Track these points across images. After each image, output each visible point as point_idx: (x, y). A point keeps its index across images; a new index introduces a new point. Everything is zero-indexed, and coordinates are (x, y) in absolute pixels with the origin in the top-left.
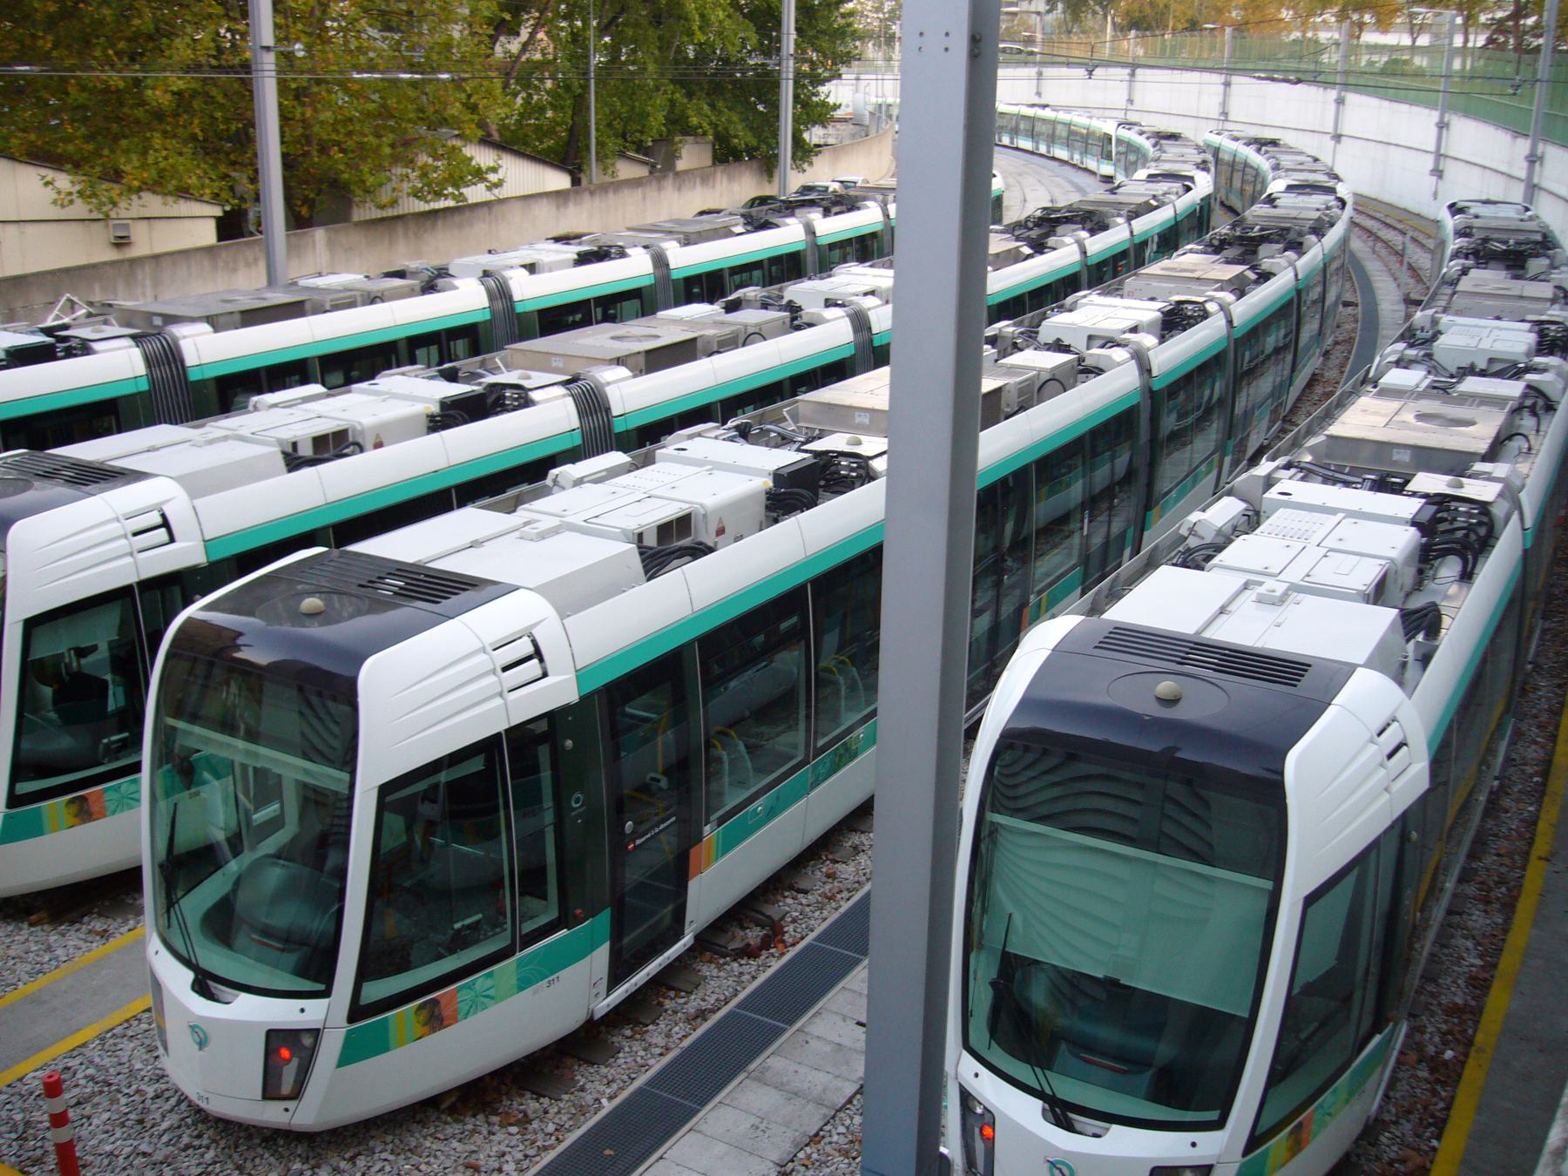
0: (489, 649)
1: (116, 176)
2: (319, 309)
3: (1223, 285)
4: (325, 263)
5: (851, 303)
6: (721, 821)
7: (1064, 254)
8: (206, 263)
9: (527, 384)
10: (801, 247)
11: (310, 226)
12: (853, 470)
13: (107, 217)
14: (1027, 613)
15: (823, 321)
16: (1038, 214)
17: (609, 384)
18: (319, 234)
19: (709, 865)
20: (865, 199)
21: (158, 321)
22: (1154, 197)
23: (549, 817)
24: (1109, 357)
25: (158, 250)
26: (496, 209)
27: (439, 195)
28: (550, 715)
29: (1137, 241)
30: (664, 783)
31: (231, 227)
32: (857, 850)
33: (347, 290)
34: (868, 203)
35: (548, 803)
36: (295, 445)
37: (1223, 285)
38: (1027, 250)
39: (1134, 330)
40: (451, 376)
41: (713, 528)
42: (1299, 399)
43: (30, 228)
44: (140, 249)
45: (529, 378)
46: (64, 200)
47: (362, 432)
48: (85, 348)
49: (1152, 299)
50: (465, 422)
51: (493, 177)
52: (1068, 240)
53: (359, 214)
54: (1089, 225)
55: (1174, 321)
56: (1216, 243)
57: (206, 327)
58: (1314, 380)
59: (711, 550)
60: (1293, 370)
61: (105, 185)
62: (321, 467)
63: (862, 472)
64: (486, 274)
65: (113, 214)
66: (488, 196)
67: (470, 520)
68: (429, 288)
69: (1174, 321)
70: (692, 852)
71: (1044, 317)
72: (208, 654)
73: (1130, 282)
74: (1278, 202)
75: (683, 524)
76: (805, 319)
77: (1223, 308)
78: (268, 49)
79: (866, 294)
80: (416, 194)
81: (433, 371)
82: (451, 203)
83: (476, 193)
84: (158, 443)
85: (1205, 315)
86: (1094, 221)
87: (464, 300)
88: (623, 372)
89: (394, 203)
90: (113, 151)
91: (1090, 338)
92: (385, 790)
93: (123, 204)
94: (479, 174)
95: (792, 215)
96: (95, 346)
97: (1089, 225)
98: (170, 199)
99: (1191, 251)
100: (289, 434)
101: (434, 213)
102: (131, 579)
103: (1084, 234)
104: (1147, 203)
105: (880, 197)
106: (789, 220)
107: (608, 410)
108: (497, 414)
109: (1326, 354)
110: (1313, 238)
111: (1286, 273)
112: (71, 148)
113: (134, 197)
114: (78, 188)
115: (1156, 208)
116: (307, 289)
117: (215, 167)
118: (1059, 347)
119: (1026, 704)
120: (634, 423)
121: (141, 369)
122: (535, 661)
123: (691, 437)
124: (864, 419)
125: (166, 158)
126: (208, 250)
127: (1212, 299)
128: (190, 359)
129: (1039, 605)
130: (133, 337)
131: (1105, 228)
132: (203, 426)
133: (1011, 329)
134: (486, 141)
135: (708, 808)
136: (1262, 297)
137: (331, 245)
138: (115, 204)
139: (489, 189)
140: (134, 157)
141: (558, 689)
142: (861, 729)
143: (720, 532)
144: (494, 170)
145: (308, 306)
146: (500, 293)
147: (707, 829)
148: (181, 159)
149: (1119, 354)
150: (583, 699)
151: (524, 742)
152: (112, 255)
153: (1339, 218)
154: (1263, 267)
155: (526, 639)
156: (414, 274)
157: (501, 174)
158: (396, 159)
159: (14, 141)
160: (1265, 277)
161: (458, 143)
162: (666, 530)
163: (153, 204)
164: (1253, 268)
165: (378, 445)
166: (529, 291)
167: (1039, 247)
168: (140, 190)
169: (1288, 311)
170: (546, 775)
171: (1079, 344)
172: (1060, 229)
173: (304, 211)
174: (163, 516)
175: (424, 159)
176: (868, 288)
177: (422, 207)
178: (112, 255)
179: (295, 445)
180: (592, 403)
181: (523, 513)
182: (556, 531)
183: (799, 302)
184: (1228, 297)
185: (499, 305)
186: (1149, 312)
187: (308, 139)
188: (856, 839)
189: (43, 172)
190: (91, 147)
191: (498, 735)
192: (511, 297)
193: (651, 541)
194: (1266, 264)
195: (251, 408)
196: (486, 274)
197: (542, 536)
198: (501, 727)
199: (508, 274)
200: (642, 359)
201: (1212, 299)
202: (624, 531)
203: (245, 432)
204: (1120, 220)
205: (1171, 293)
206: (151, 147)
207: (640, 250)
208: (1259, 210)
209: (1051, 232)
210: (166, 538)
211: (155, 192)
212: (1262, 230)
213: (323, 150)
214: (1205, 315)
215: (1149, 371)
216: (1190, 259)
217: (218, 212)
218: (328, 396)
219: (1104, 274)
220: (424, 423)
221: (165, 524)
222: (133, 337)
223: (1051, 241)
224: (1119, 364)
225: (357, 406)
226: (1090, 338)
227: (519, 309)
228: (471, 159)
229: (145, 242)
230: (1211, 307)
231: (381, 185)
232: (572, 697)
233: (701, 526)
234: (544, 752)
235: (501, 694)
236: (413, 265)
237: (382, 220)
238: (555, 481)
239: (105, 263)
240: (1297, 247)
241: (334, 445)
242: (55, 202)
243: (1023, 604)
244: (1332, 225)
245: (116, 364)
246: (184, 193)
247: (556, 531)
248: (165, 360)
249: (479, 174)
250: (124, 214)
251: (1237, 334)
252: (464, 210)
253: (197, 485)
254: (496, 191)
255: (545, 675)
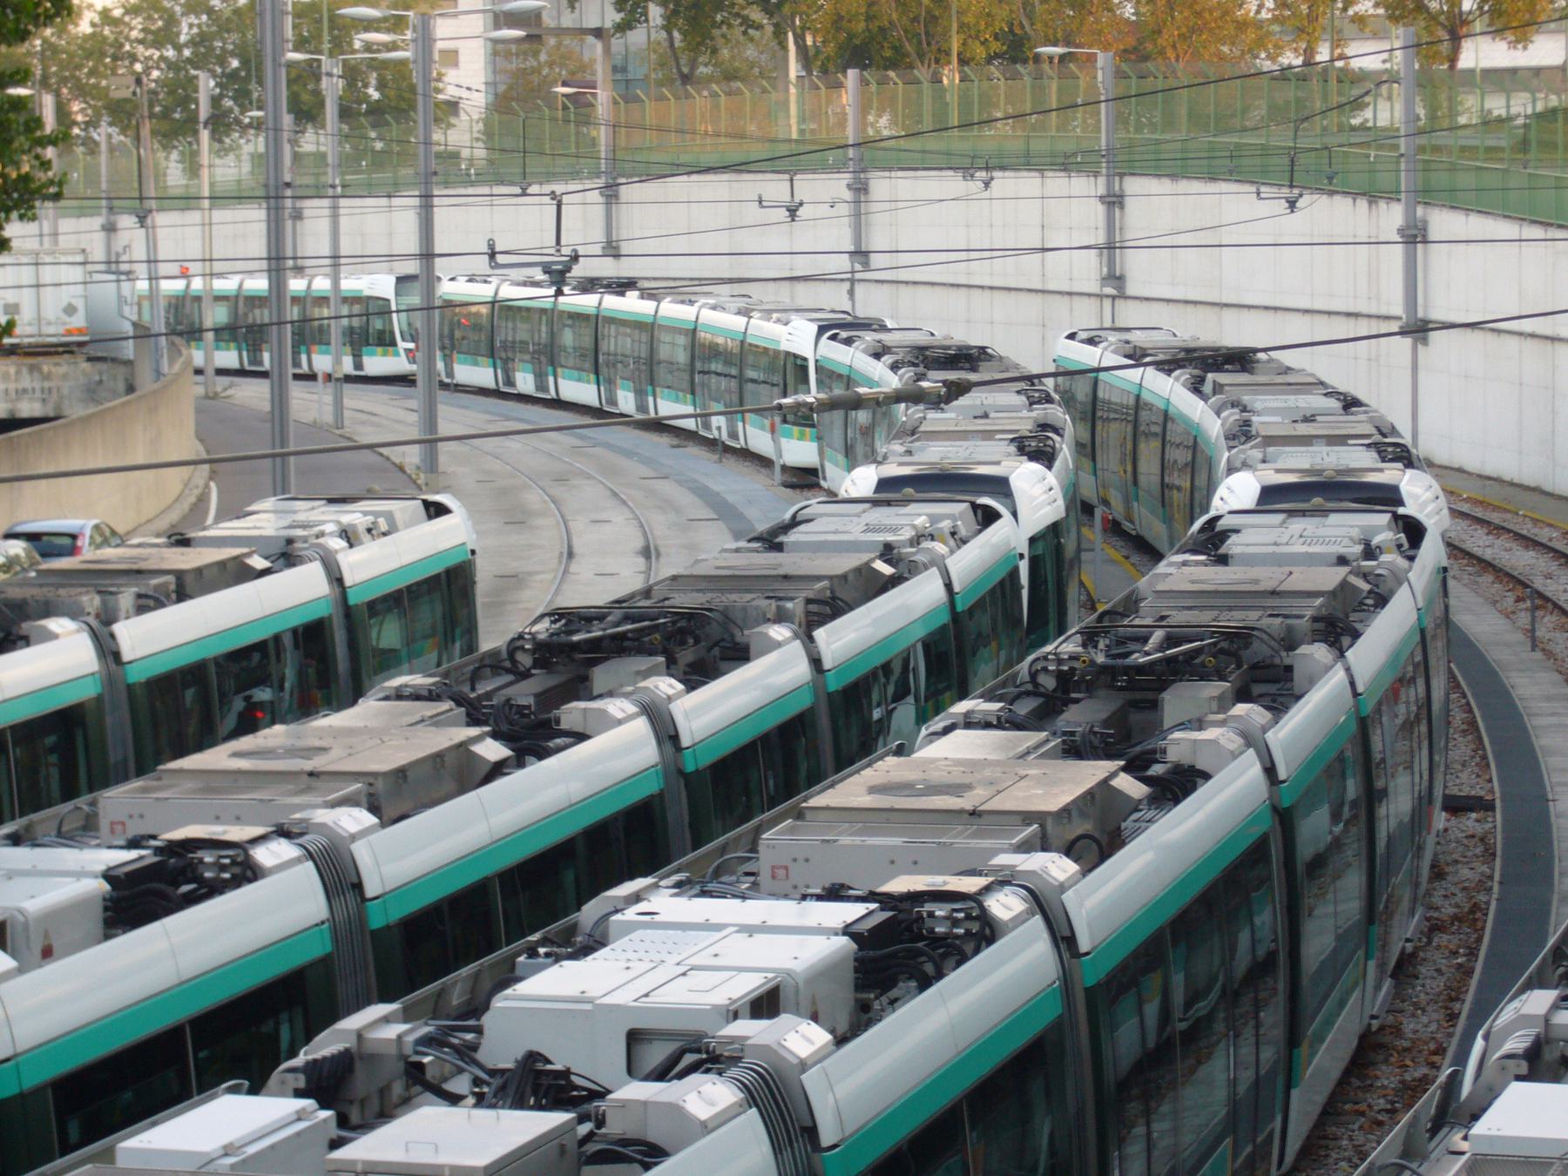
3: (1044, 832)
7: (610, 751)
16: (543, 629)
20: (48, 610)
22: (888, 552)
24: (676, 1111)
29: (834, 684)
34: (55, 624)
37: (1044, 832)
38: (492, 750)
39: (766, 1004)
42: (1330, 1112)
49: (835, 893)
52: (617, 707)
54: (686, 656)
55: (900, 951)
56: (1049, 683)
58: (1369, 1049)
60: (1293, 1038)
69: (900, 951)
71: (508, 977)
73: (778, 839)
74: (1233, 545)
77: (1043, 903)
85: (986, 932)
86: (697, 639)
91: (635, 1038)
97: (686, 656)
99: (969, 723)
103: (666, 685)
104: (865, 571)
105: (91, 602)
109: (1404, 969)
110: (1319, 652)
111: (1237, 764)
115: (894, 581)
118: (536, 1083)
127: (1005, 880)
131: (741, 655)
133: (392, 1031)
136: (1168, 848)
149: (706, 1096)
153: (1400, 579)
154: (1173, 755)
160: (1178, 784)
164: (1136, 767)
167: (533, 737)
169: (1258, 873)
171: (591, 1058)
172: (601, 676)
184: (1058, 867)
186: (804, 936)
194: (1179, 745)
201: (1005, 880)
204: (779, 632)
205: (894, 867)
208: (1180, 572)
209: (578, 688)
212: (1171, 641)
214: (986, 932)
215: (812, 1132)
216: (960, 751)
219: (699, 819)
223: (572, 713)
224: (706, 1128)
226: (635, 1038)
230: (1004, 905)
240: (1272, 684)
244: (1382, 601)
251: (1091, 974)
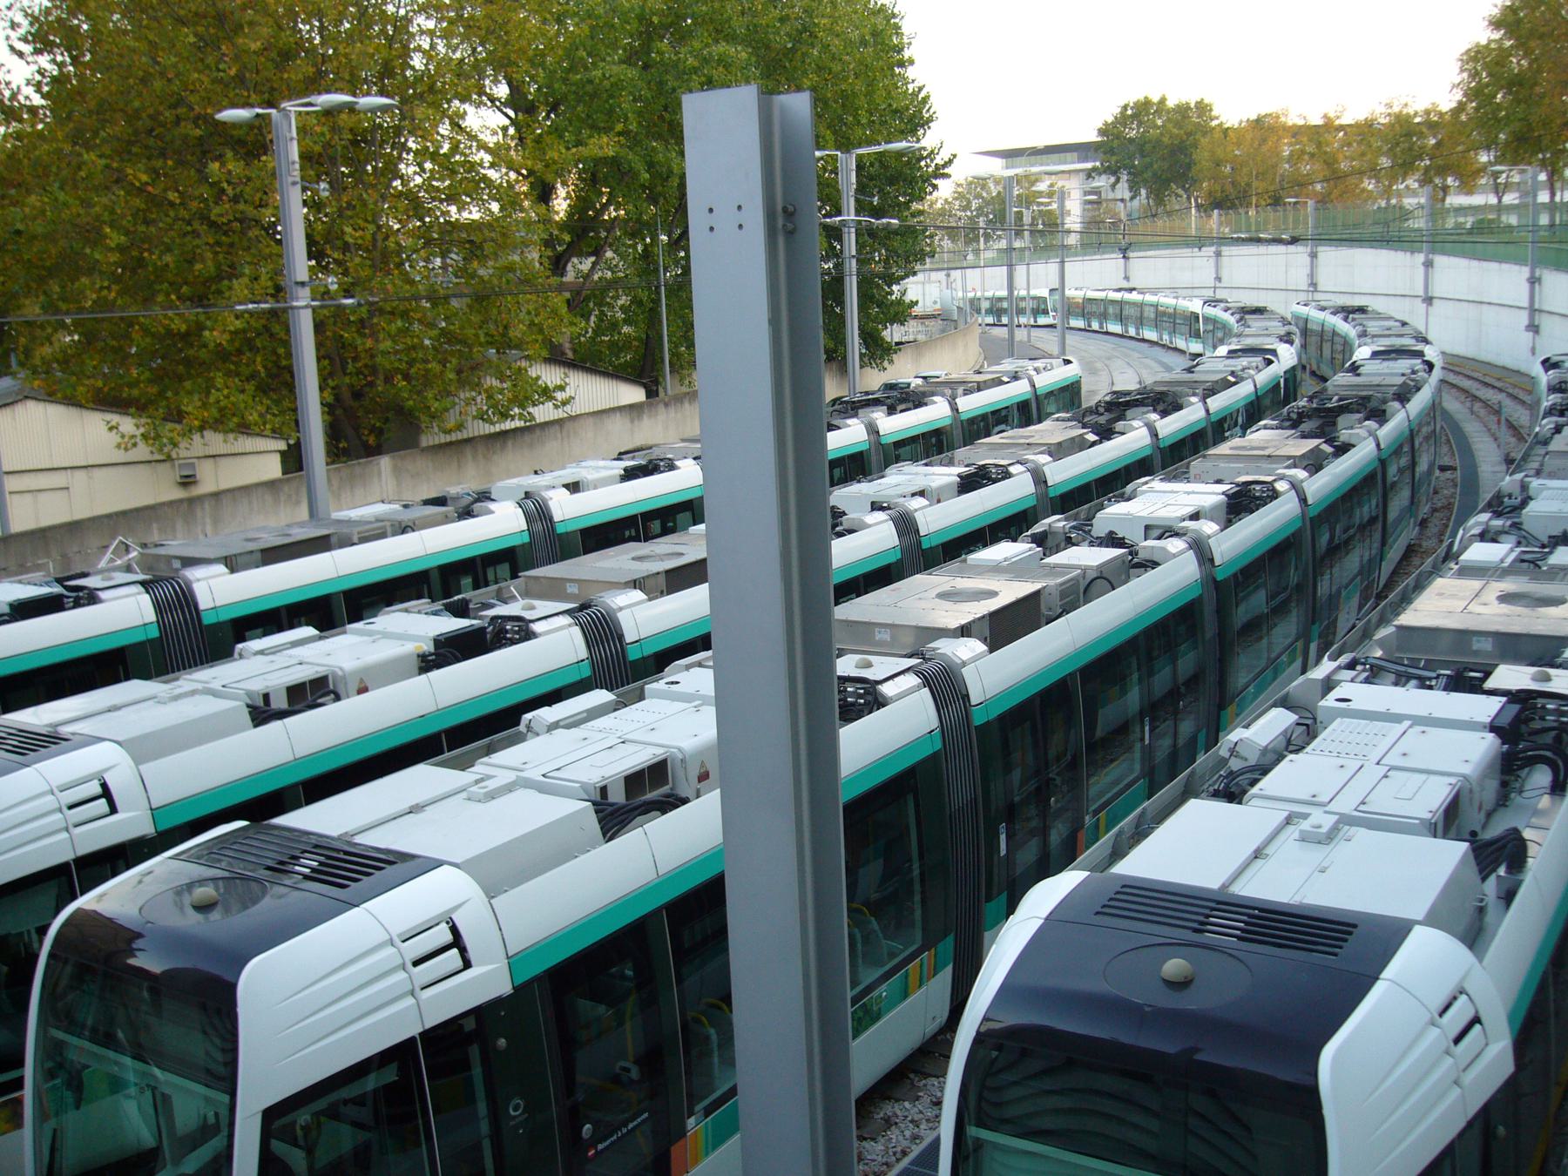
0: (397, 941)
1: (177, 416)
2: (346, 542)
3: (1295, 462)
4: (377, 492)
5: (897, 505)
6: (708, 1112)
7: (1133, 438)
8: (268, 498)
9: (528, 615)
10: (865, 447)
11: (380, 453)
12: (860, 696)
13: (169, 458)
14: (1082, 836)
15: (866, 526)
16: (1108, 398)
17: (621, 609)
18: (385, 462)
19: (696, 1162)
20: (933, 394)
21: (177, 564)
22: (1233, 373)
23: (484, 1127)
24: (1164, 549)
25: (224, 485)
26: (568, 425)
27: (505, 416)
28: (477, 1012)
29: (1214, 419)
30: (635, 1073)
31: (294, 460)
32: (889, 1123)
33: (378, 520)
34: (935, 398)
35: (482, 1108)
36: (266, 697)
37: (1295, 462)
38: (1092, 437)
39: (1195, 516)
40: (460, 610)
41: (694, 773)
42: (1395, 573)
43: (97, 473)
44: (207, 486)
45: (533, 608)
46: (128, 444)
47: (344, 677)
48: (91, 598)
49: (1218, 482)
50: (459, 661)
51: (560, 396)
52: (1136, 423)
53: (426, 440)
54: (1160, 407)
55: (1241, 503)
56: (1294, 416)
57: (221, 568)
58: (1410, 551)
59: (685, 801)
60: (1383, 543)
61: (170, 426)
62: (287, 721)
63: (870, 698)
64: (528, 495)
65: (174, 455)
66: (560, 414)
67: (422, 779)
68: (466, 513)
69: (1241, 503)
70: (675, 1150)
71: (1102, 507)
72: (100, 947)
73: (1196, 464)
74: (1361, 370)
75: (658, 772)
76: (846, 525)
77: (1295, 486)
78: (303, 284)
79: (913, 495)
80: (482, 417)
81: (438, 606)
82: (518, 423)
83: (544, 412)
84: (117, 701)
85: (1274, 495)
86: (1164, 401)
87: (502, 523)
88: (638, 595)
89: (460, 427)
90: (176, 393)
91: (1147, 528)
92: (272, 1116)
93: (182, 445)
94: (547, 393)
95: (856, 416)
96: (102, 595)
97: (1160, 407)
98: (231, 436)
99: (1265, 427)
100: (258, 686)
101: (504, 434)
102: (67, 856)
103: (1154, 416)
104: (1225, 380)
105: (948, 392)
106: (849, 421)
107: (621, 637)
108: (499, 648)
109: (1423, 524)
110: (1396, 405)
111: (1365, 445)
112: (135, 392)
113: (197, 437)
114: (142, 430)
115: (1235, 384)
116: (339, 522)
117: (277, 402)
118: (1112, 540)
119: (1007, 991)
120: (649, 650)
121: (150, 615)
122: (455, 951)
123: (688, 667)
124: (885, 636)
125: (227, 397)
126: (271, 485)
127: (1282, 477)
128: (204, 602)
129: (1097, 826)
130: (143, 583)
131: (1179, 408)
132: (177, 679)
133: (1061, 524)
134: (556, 357)
135: (690, 1096)
136: (1340, 471)
137: (397, 471)
138: (175, 445)
139: (556, 407)
140: (196, 397)
141: (487, 980)
142: (884, 986)
143: (704, 777)
144: (561, 388)
145: (334, 540)
146: (538, 513)
147: (691, 1121)
148: (241, 396)
149: (1175, 545)
150: (519, 990)
151: (448, 1045)
152: (179, 494)
153: (1425, 381)
154: (1342, 439)
155: (444, 925)
156: (456, 498)
157: (569, 392)
158: (462, 383)
159: (81, 389)
160: (1342, 449)
161: (524, 364)
162: (635, 781)
163: (215, 441)
164: (1329, 441)
165: (363, 690)
166: (567, 509)
167: (1106, 433)
168: (202, 429)
169: (1370, 483)
170: (477, 1071)
171: (1134, 535)
172: (1129, 413)
173: (372, 440)
174: (104, 786)
175: (491, 382)
176: (916, 489)
177: (489, 429)
178: (179, 494)
179: (266, 697)
180: (601, 631)
181: (480, 768)
182: (509, 788)
183: (842, 507)
184: (1301, 474)
185: (538, 527)
186: (1210, 495)
187: (374, 370)
188: (888, 1109)
189: (109, 416)
190: (154, 390)
191: (412, 1039)
192: (551, 519)
193: (617, 796)
194: (1344, 435)
195: (236, 655)
196: (528, 495)
197: (492, 796)
198: (414, 1030)
199: (548, 494)
200: (662, 579)
201: (1282, 477)
202: (584, 786)
203: (216, 685)
204: (1194, 399)
205: (1239, 474)
206: (214, 387)
207: (690, 461)
208: (1341, 379)
209: (1122, 417)
210: (106, 809)
211: (216, 430)
212: (1340, 400)
213: (388, 379)
214: (1274, 495)
215: (1212, 560)
216: (1263, 436)
217: (282, 446)
218: (321, 638)
219: (1171, 458)
220: (415, 663)
221: (106, 793)
222: (143, 583)
223: (1119, 426)
224: (1175, 556)
225: (345, 651)
226: (1147, 528)
227: (560, 529)
228: (538, 378)
229: (211, 479)
230: (1281, 486)
231: (447, 410)
232: (505, 988)
233: (680, 773)
234: (474, 1052)
235: (412, 993)
236: (453, 490)
237: (451, 444)
238: (529, 727)
239: (163, 504)
240: (1380, 416)
241: (311, 693)
242: (119, 446)
243: (1077, 827)
244: (1418, 389)
245: (124, 611)
246: (244, 429)
247: (509, 788)
248: (176, 604)
249: (547, 393)
250: (183, 454)
251: (1312, 512)
252: (533, 429)
253: (142, 749)
254: (568, 408)
255: (467, 964)
